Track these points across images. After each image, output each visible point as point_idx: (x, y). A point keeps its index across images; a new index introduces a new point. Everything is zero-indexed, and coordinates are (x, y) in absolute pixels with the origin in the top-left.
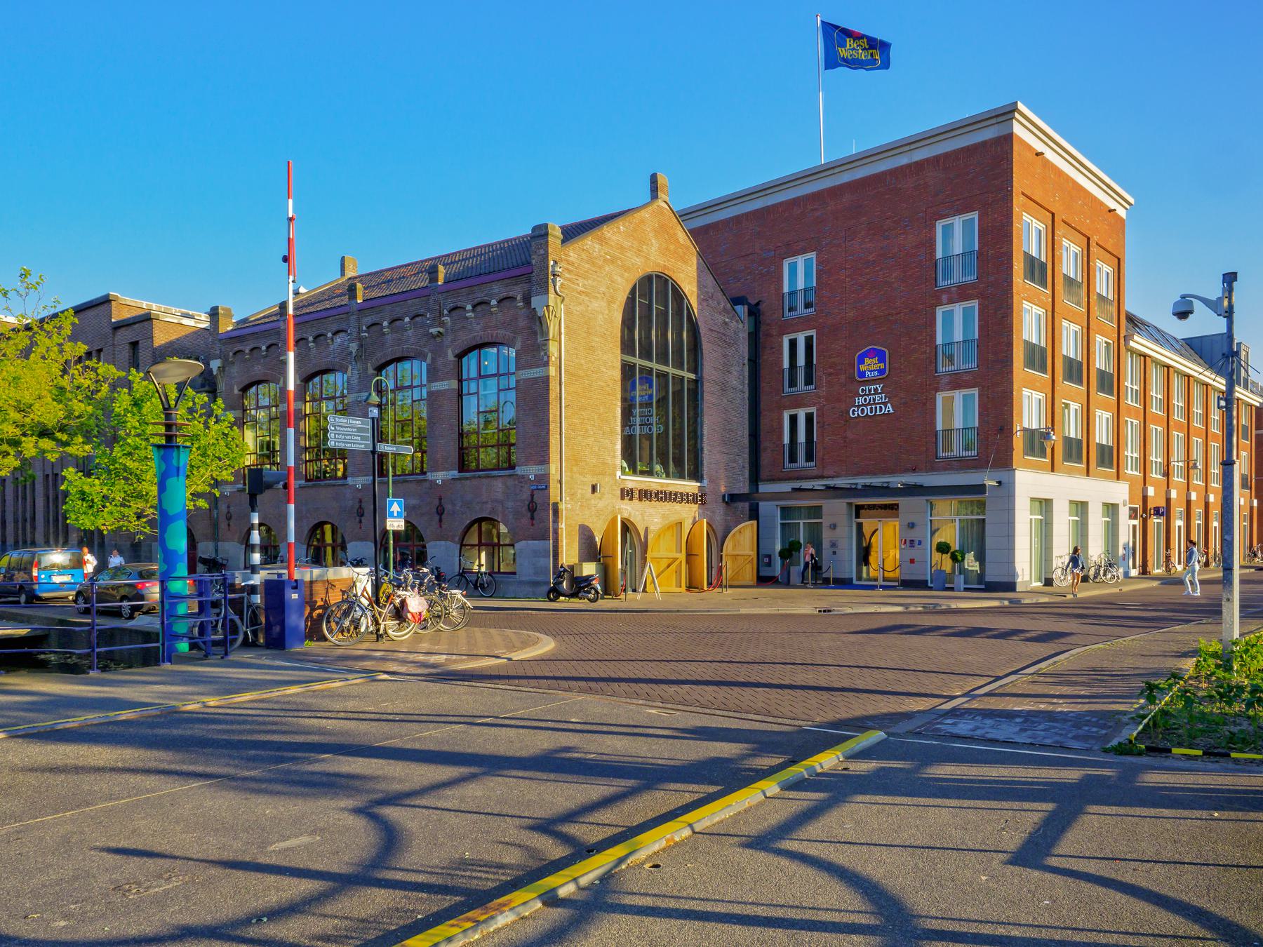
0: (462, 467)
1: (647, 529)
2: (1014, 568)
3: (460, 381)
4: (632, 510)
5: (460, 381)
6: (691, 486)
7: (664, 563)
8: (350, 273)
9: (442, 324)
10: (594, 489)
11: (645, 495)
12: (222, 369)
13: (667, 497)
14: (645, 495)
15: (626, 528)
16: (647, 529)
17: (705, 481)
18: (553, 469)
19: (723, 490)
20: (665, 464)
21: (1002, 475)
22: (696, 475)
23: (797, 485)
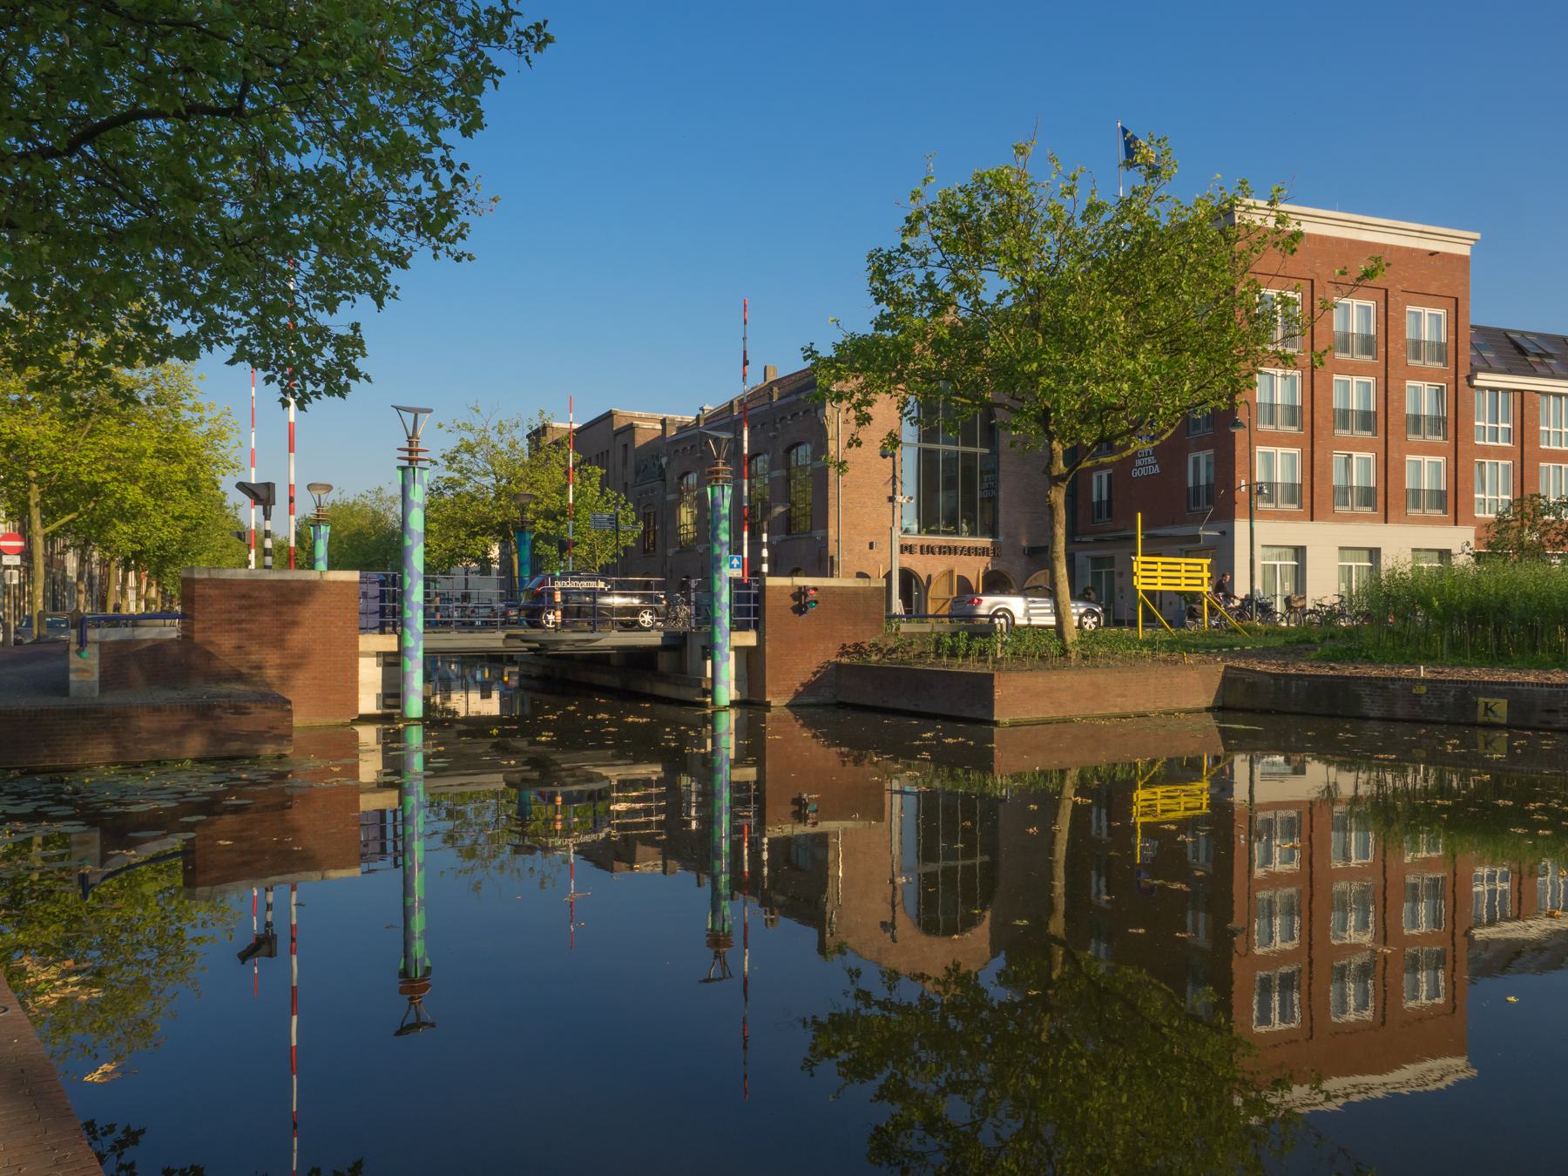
0: (788, 532)
1: (929, 577)
2: (1014, 595)
3: (788, 470)
4: (921, 565)
5: (788, 470)
6: (985, 542)
7: (940, 603)
8: (770, 379)
9: (775, 430)
10: (871, 546)
11: (929, 550)
12: (668, 463)
13: (969, 551)
14: (929, 550)
15: (907, 576)
16: (929, 577)
17: (1001, 538)
18: (832, 532)
19: (1024, 544)
20: (971, 521)
21: (1223, 526)
22: (992, 531)
23: (1100, 536)
